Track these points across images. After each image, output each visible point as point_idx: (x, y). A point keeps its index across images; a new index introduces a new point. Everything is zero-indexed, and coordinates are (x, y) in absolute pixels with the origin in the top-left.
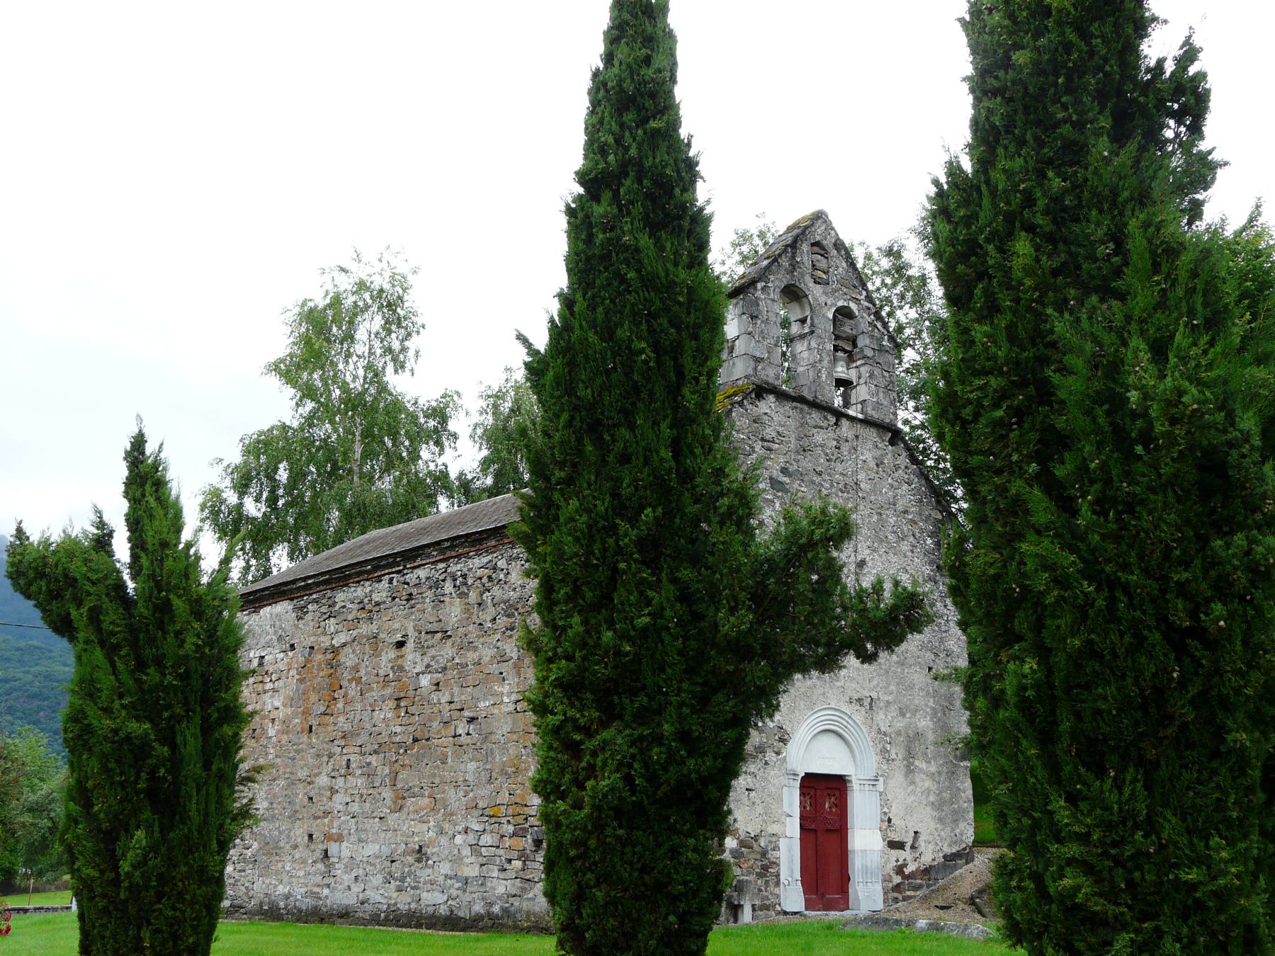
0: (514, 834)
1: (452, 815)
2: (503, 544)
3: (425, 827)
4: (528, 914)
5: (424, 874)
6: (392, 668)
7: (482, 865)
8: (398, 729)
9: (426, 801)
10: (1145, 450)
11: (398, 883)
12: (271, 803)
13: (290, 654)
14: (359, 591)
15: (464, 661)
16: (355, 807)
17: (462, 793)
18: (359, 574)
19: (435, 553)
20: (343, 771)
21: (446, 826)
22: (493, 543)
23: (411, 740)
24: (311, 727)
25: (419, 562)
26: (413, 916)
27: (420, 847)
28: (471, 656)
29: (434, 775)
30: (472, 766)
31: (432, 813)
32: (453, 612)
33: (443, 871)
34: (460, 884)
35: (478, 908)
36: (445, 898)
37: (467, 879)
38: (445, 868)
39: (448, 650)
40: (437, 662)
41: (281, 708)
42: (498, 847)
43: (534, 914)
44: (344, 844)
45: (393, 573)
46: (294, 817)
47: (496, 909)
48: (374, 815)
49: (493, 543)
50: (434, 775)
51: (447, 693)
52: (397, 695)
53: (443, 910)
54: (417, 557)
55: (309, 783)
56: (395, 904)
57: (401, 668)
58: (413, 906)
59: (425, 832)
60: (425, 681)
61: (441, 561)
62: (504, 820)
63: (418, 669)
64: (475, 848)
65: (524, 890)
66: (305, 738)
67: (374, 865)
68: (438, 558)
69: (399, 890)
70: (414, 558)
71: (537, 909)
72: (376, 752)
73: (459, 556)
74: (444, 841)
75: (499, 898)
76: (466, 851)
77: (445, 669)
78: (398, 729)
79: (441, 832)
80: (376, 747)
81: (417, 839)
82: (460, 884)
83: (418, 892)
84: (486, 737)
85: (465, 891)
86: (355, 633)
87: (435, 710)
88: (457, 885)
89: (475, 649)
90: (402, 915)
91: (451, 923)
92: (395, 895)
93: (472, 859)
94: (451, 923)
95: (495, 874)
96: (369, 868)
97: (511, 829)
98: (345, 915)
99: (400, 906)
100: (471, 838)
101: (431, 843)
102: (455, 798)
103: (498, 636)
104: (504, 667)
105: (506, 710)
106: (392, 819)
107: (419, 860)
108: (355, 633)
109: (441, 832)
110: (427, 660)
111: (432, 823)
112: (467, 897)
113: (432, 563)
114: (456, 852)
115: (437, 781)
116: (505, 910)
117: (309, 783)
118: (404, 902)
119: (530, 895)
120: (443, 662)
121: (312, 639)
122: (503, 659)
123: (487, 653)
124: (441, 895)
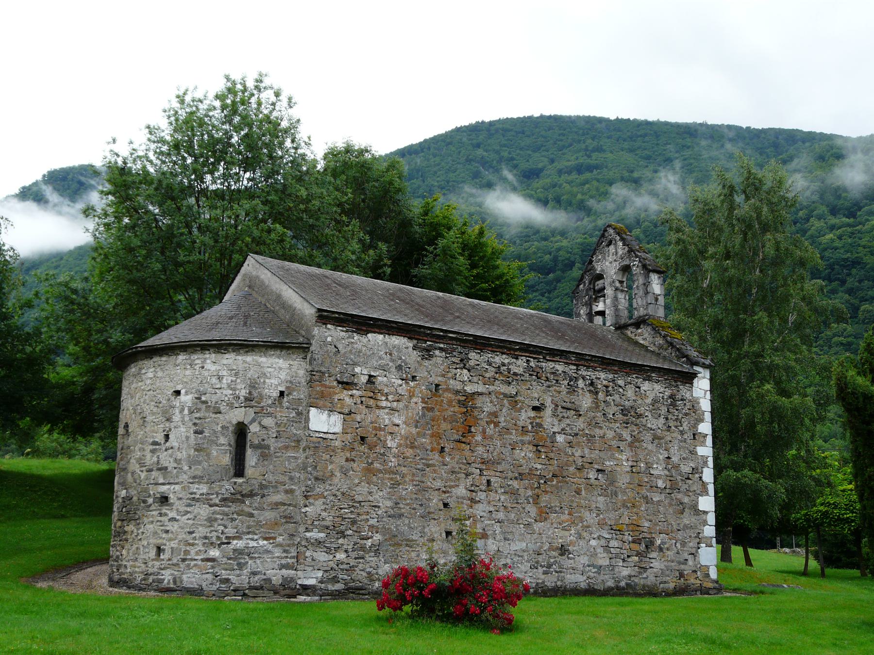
0: (634, 542)
1: (588, 527)
2: (621, 372)
3: (567, 533)
4: (644, 586)
5: (567, 563)
6: (531, 423)
7: (610, 559)
8: (539, 467)
9: (566, 517)
10: (126, 226)
11: (545, 569)
12: (397, 504)
13: (412, 384)
14: (498, 359)
15: (592, 434)
16: (501, 515)
17: (595, 515)
18: (509, 349)
19: (573, 359)
20: (484, 488)
21: (584, 534)
22: (616, 368)
23: (550, 476)
24: (443, 448)
25: (557, 358)
26: (558, 590)
27: (562, 545)
28: (598, 432)
29: (572, 501)
30: (601, 499)
31: (572, 525)
32: (585, 401)
33: (582, 562)
34: (596, 570)
35: (610, 583)
36: (585, 578)
37: (601, 567)
38: (584, 560)
39: (580, 424)
40: (571, 429)
41: (402, 426)
42: (621, 549)
43: (648, 586)
44: (490, 541)
45: (531, 357)
46: (427, 516)
47: (623, 584)
48: (520, 522)
49: (616, 368)
50: (572, 501)
51: (579, 451)
52: (535, 442)
53: (583, 585)
54: (557, 355)
55: (444, 492)
56: (543, 582)
57: (540, 425)
58: (559, 583)
59: (569, 536)
60: (560, 438)
61: (574, 365)
62: (626, 533)
63: (556, 429)
64: (607, 548)
65: (640, 573)
66: (436, 456)
67: (522, 556)
68: (573, 362)
69: (545, 573)
70: (554, 355)
71: (649, 583)
72: (516, 478)
73: (588, 367)
74: (581, 543)
75: (624, 578)
76: (600, 550)
77: (576, 435)
78: (539, 467)
79: (580, 537)
80: (517, 475)
81: (561, 541)
82: (596, 570)
83: (563, 574)
84: (612, 482)
85: (599, 574)
86: (492, 388)
87: (570, 459)
88: (594, 570)
89: (601, 428)
90: (549, 590)
91: (590, 592)
92: (543, 577)
93: (605, 555)
94: (590, 592)
95: (621, 564)
96: (516, 559)
97: (630, 539)
98: (577, 592)
99: (548, 584)
100: (603, 542)
101: (572, 543)
102: (590, 518)
103: (618, 425)
104: (622, 445)
105: (626, 470)
106: (537, 526)
107: (562, 555)
108: (492, 388)
109: (580, 537)
110: (563, 425)
111: (573, 532)
112: (601, 577)
113: (566, 363)
114: (592, 550)
115: (575, 505)
116: (627, 584)
117: (444, 492)
118: (550, 581)
119: (645, 576)
120: (576, 430)
121: (440, 379)
122: (621, 439)
123: (610, 434)
124: (581, 576)
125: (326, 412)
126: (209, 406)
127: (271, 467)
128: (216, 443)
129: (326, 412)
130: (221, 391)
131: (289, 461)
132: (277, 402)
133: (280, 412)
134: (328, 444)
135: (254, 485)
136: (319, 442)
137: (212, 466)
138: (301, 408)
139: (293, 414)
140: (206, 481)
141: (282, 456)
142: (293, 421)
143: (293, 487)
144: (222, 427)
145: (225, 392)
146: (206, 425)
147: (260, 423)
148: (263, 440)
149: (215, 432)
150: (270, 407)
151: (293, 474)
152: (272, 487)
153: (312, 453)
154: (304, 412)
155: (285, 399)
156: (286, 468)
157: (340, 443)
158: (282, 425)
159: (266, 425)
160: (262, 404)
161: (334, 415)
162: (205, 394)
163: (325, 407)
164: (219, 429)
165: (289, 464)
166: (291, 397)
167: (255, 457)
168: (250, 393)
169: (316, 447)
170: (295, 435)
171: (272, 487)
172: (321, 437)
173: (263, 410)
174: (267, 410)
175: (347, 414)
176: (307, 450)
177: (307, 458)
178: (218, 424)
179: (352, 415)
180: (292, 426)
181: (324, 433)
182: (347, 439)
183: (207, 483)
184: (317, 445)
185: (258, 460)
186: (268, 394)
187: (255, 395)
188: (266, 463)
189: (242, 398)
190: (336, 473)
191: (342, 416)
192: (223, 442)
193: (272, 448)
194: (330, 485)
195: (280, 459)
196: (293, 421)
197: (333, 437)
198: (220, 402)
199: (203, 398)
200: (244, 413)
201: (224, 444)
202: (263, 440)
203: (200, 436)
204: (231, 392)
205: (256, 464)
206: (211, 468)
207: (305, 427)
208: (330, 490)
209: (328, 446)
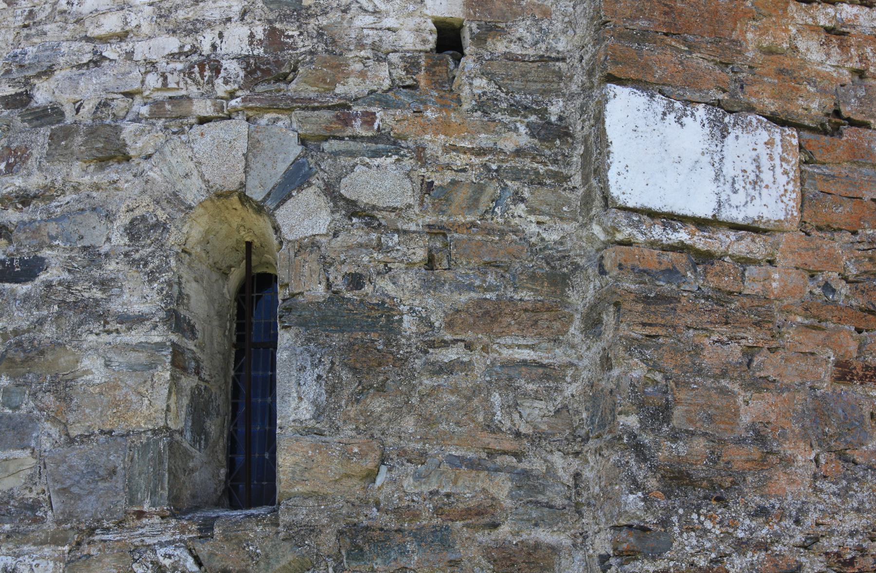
125: (701, 112)
126: (68, 132)
127: (409, 424)
128: (103, 317)
129: (701, 112)
130: (126, 46)
131: (509, 385)
132: (422, 78)
133: (444, 127)
134: (727, 283)
135: (312, 530)
136: (671, 273)
137: (86, 438)
138: (555, 109)
139: (522, 138)
140: (50, 526)
141: (466, 366)
142: (517, 174)
143: (544, 535)
144: (133, 231)
145: (141, 50)
146: (52, 228)
147: (331, 192)
148: (356, 281)
149: (93, 256)
150: (386, 105)
151: (536, 465)
152: (419, 536)
153: (638, 332)
154: (579, 128)
155: (468, 63)
156: (491, 428)
157: (796, 279)
158: (461, 196)
159: (365, 198)
160: (350, 87)
161: (747, 127)
162: (49, 72)
163: (693, 81)
164: (119, 240)
165: (512, 407)
166: (500, 47)
167: (309, 376)
168: (274, 37)
169: (661, 299)
170: (537, 249)
171: (419, 536)
172: (681, 248)
173: (346, 122)
174: (369, 119)
175: (820, 130)
176: (609, 318)
177: (606, 363)
178: (109, 217)
179: (849, 134)
180: (518, 198)
181: (701, 223)
182: (832, 259)
183: (56, 541)
184: (664, 286)
185: (332, 391)
186: (372, 36)
187: (304, 45)
188: (377, 405)
189: (232, 67)
190: (787, 449)
191: (793, 137)
192: (138, 308)
193: (409, 324)
194: (762, 512)
195: (458, 378)
196: (517, 174)
197: (743, 246)
198: (120, 103)
199: (42, 96)
200: (242, 145)
201: (140, 319)
202: (356, 281)
203: (22, 289)
204: (172, 44)
205: (319, 413)
206: (75, 457)
207: (587, 201)
208: (762, 546)
209: (722, 297)
